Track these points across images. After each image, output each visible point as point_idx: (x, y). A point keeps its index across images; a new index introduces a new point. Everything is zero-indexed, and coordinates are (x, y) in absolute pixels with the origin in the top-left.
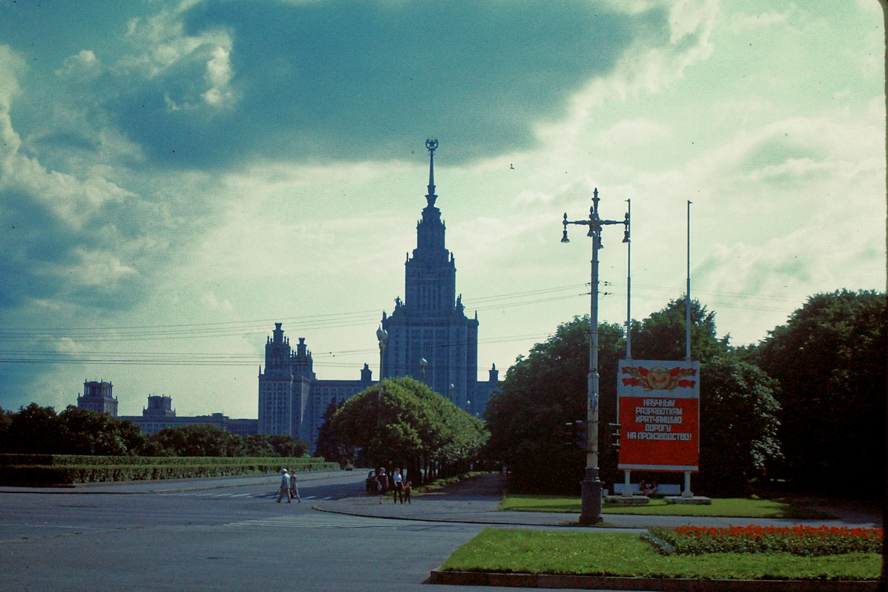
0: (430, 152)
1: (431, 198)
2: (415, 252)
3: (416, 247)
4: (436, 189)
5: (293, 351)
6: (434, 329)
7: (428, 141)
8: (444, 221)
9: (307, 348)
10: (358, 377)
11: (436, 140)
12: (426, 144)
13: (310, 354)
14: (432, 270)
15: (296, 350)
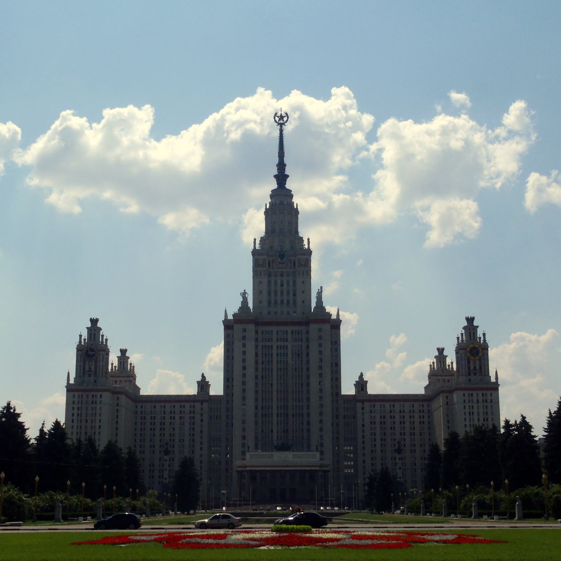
0: (279, 127)
1: (281, 178)
2: (262, 238)
3: (263, 234)
4: (286, 168)
5: (112, 364)
6: (289, 329)
7: (276, 114)
8: (297, 204)
9: (129, 361)
10: (192, 390)
11: (286, 114)
12: (274, 118)
13: (133, 370)
14: (285, 260)
15: (116, 363)
